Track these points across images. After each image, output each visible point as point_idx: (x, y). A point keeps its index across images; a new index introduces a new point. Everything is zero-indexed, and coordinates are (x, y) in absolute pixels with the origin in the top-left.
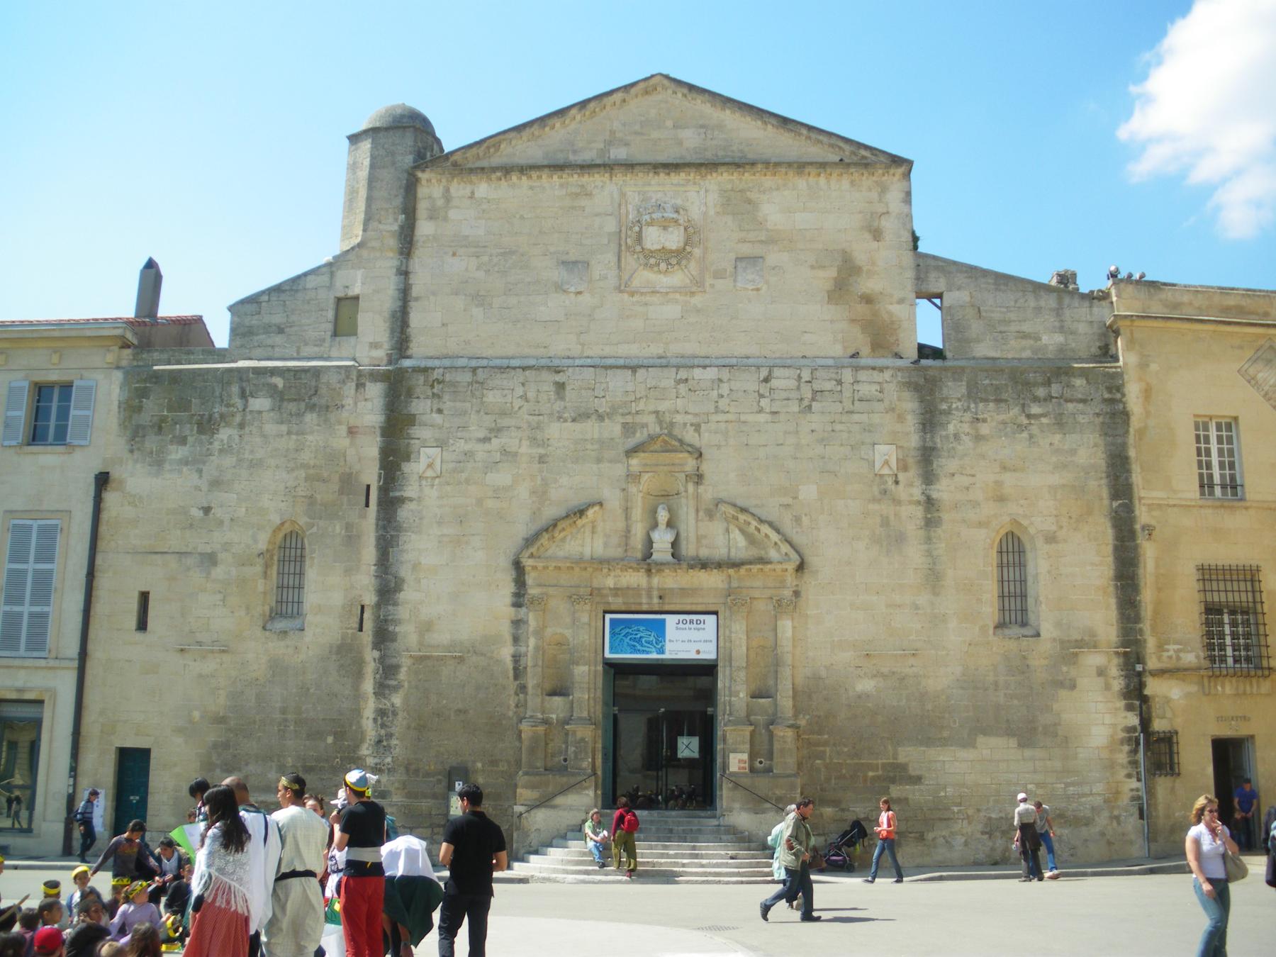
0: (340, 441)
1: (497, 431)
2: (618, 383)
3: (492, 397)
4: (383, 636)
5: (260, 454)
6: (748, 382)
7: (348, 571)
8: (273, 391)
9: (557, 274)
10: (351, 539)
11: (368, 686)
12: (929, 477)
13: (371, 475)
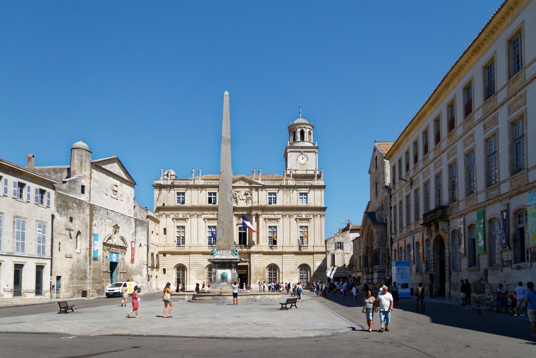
0: (85, 216)
1: (101, 219)
2: (112, 213)
3: (101, 212)
4: (90, 255)
5: (75, 216)
6: (122, 217)
7: (86, 242)
8: (77, 204)
9: (105, 191)
10: (86, 236)
11: (88, 264)
12: (135, 236)
13: (88, 224)
